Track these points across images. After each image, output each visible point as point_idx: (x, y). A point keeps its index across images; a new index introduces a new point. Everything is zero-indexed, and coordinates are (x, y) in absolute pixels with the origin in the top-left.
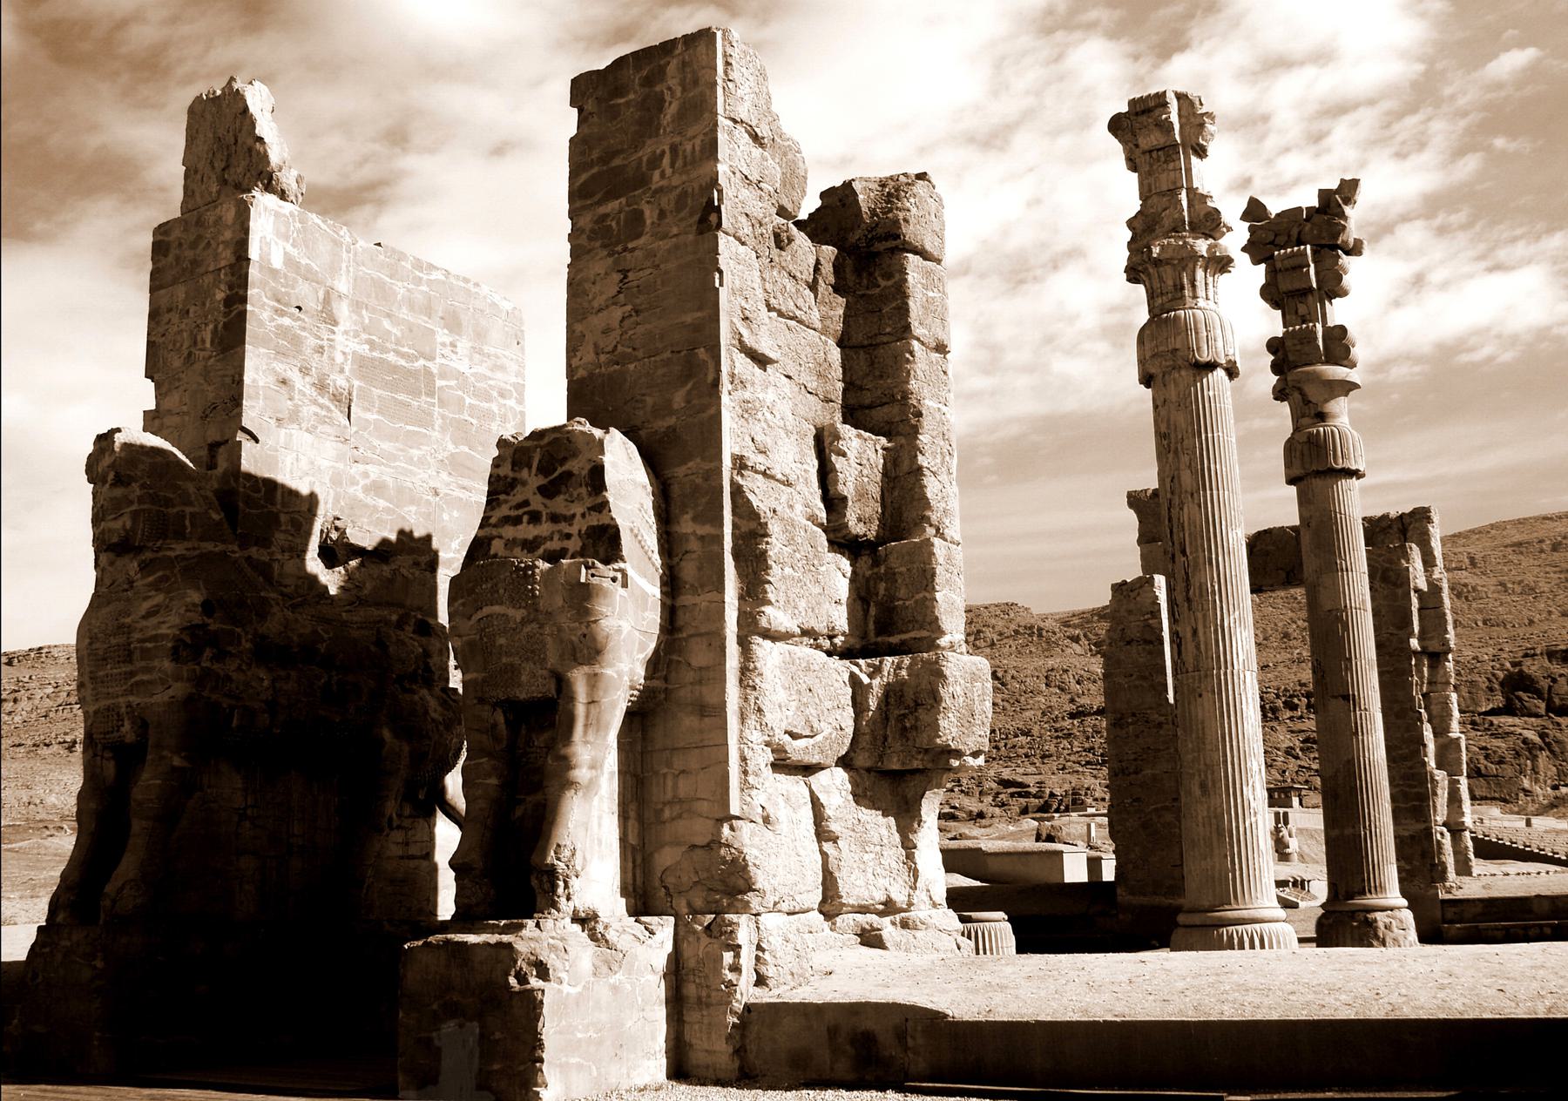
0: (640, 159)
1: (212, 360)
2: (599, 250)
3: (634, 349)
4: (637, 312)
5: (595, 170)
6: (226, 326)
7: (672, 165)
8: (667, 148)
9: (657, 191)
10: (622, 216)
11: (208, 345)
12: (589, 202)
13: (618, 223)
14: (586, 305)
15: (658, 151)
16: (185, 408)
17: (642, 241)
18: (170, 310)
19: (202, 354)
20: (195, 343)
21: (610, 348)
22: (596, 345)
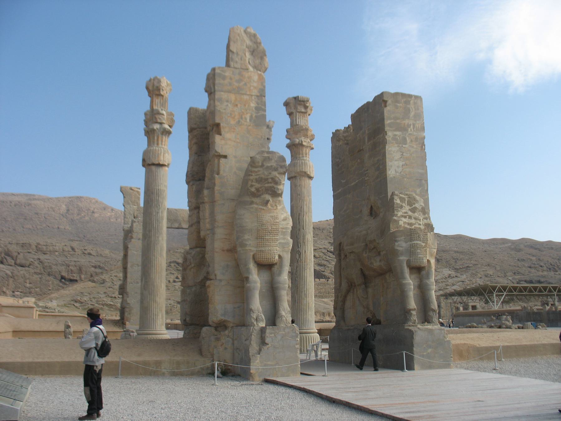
0: (405, 123)
5: (392, 121)
6: (256, 116)
7: (413, 129)
8: (412, 124)
9: (410, 134)
11: (248, 120)
12: (391, 129)
13: (400, 138)
15: (410, 123)
16: (238, 141)
17: (407, 146)
18: (227, 101)
19: (245, 123)
20: (242, 118)
21: (400, 172)
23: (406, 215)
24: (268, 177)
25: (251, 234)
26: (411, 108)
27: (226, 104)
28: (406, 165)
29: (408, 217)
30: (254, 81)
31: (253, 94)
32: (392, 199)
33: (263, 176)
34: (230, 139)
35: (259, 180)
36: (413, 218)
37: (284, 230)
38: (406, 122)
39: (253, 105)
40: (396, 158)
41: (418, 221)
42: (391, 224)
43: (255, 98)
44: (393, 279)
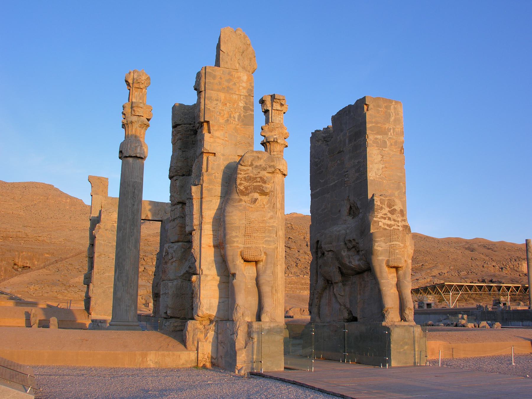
0: (385, 127)
1: (239, 126)
2: (376, 147)
3: (386, 177)
4: (386, 168)
5: (373, 125)
7: (393, 133)
8: (392, 128)
9: (390, 138)
10: (381, 140)
11: (236, 120)
13: (380, 141)
14: (372, 160)
16: (226, 139)
17: (387, 149)
18: (217, 100)
19: (234, 122)
20: (230, 117)
21: (379, 174)
22: (375, 172)
23: (386, 216)
24: (257, 176)
25: (239, 231)
26: (392, 112)
27: (215, 102)
28: (386, 168)
29: (387, 218)
30: (243, 81)
31: (242, 94)
32: (372, 199)
33: (252, 175)
34: (218, 137)
35: (249, 179)
36: (392, 219)
37: (271, 228)
38: (387, 126)
39: (241, 104)
40: (376, 161)
41: (397, 223)
42: (371, 225)
43: (244, 98)
44: (372, 279)
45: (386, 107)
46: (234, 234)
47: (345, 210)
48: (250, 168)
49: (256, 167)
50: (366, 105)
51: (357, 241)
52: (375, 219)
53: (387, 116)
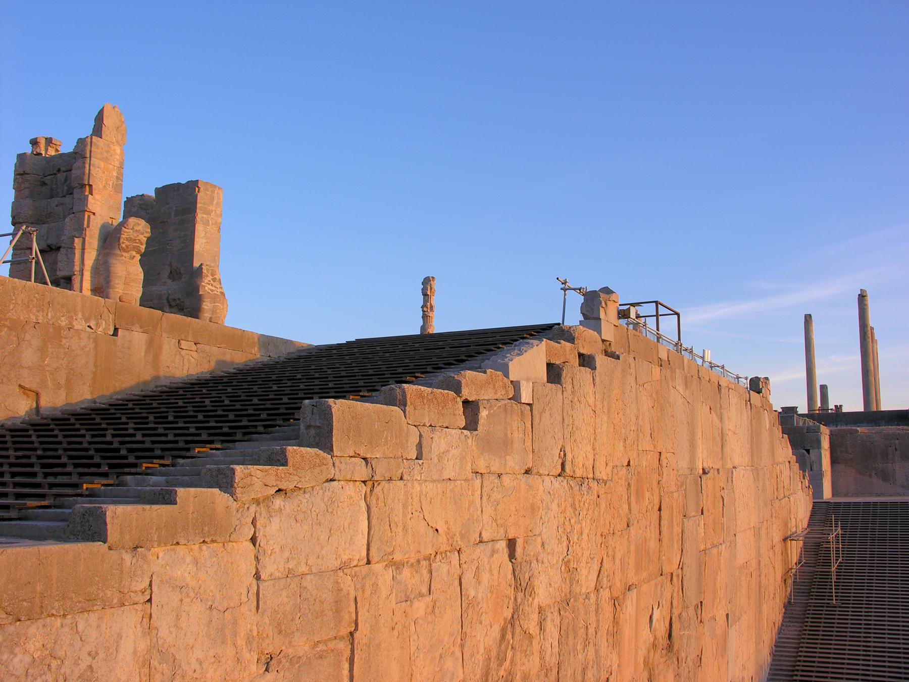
18: (99, 168)
27: (97, 169)
33: (132, 237)
35: (129, 239)
38: (211, 208)
39: (115, 174)
40: (201, 236)
45: (212, 191)
46: (117, 281)
47: (165, 273)
48: (132, 231)
49: (136, 231)
50: (198, 187)
51: (182, 300)
52: (203, 284)
53: (212, 199)
